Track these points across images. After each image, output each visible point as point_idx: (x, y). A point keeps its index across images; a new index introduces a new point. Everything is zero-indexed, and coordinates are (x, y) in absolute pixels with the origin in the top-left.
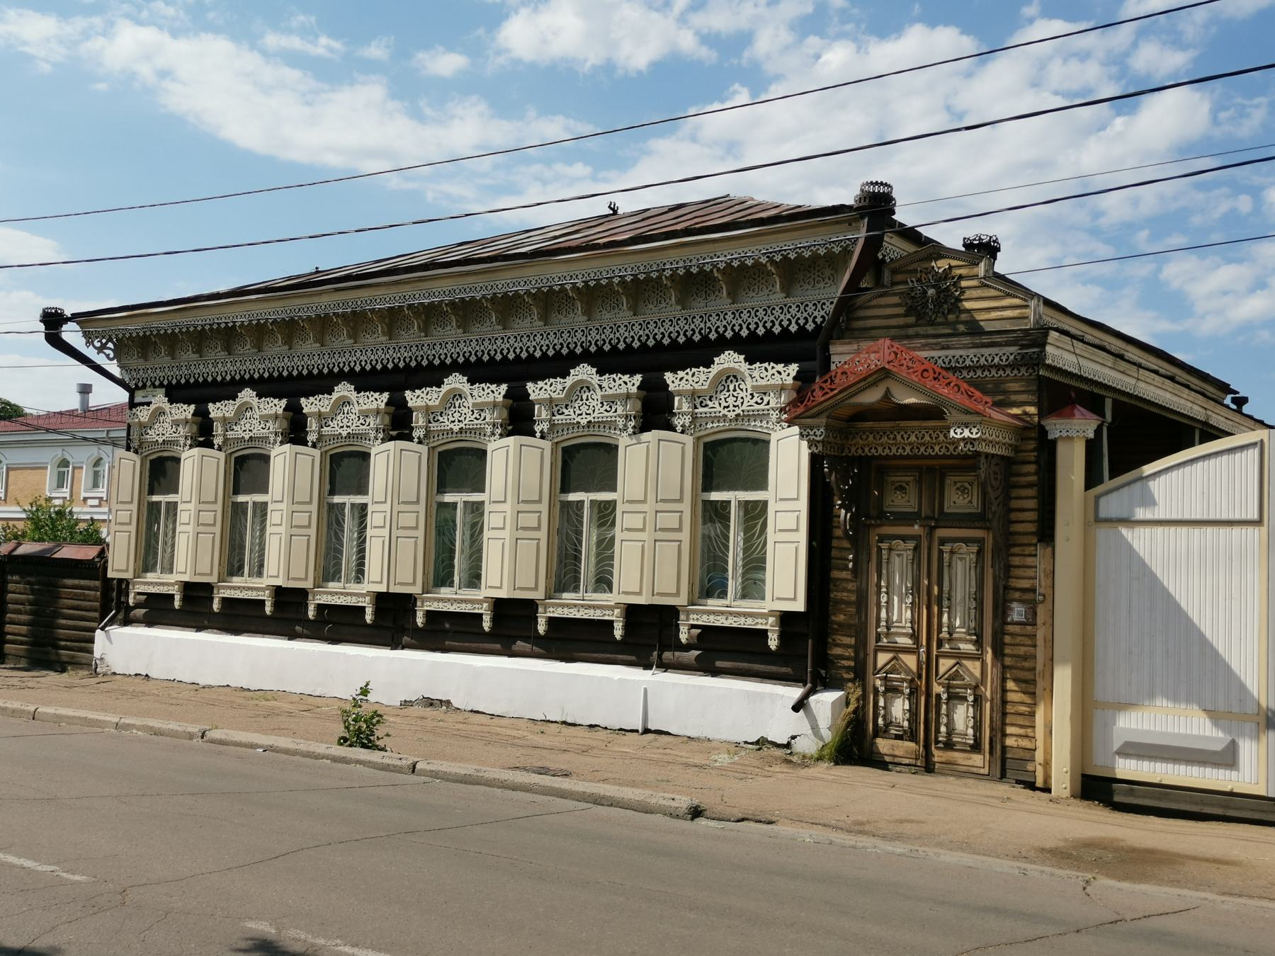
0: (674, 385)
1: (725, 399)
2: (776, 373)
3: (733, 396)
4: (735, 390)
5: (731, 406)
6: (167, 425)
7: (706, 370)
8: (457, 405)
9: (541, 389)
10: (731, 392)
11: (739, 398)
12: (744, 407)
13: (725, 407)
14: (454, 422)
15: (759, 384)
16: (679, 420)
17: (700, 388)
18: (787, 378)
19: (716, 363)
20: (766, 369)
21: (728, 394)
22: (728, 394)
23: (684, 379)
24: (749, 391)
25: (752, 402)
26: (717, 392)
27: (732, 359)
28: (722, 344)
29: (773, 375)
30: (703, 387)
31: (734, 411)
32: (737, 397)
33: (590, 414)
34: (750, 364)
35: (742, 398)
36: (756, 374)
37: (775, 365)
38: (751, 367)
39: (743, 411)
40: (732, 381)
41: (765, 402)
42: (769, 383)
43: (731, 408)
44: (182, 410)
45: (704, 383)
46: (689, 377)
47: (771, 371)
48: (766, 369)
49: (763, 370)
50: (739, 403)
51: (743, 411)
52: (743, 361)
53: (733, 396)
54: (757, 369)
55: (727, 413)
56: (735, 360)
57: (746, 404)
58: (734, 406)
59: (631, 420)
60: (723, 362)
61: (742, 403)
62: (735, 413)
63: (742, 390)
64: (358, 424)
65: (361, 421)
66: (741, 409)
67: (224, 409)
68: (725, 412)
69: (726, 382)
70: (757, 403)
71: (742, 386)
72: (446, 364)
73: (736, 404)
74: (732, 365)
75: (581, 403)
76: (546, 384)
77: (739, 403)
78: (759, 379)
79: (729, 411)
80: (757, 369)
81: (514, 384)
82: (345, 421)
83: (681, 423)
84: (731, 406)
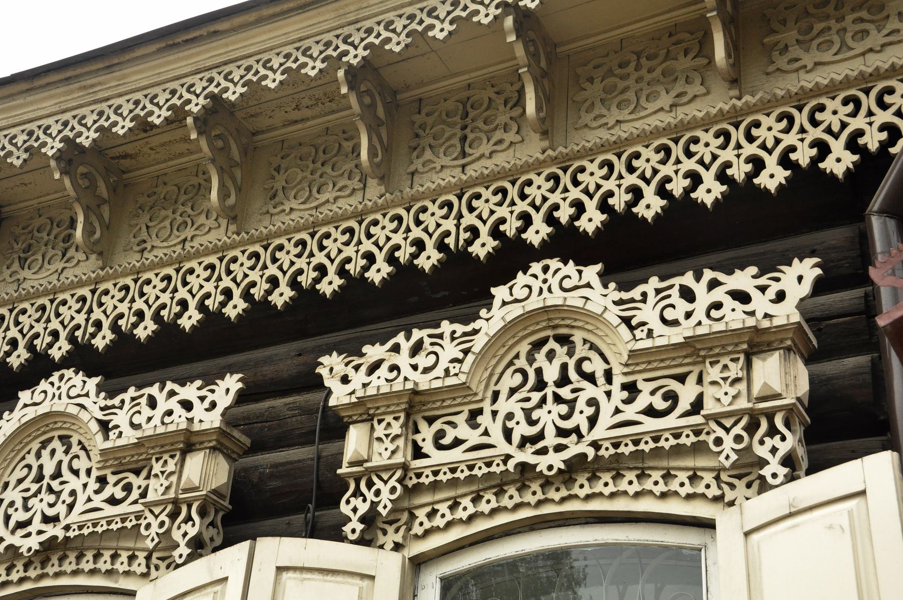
0: (349, 388)
1: (528, 413)
3: (558, 399)
4: (563, 381)
5: (550, 432)
7: (460, 329)
10: (549, 391)
11: (581, 404)
12: (600, 432)
13: (525, 441)
15: (660, 342)
17: (437, 384)
18: (773, 309)
19: (497, 303)
20: (688, 295)
21: (536, 397)
22: (536, 397)
23: (385, 367)
24: (618, 380)
25: (630, 412)
26: (496, 395)
27: (554, 282)
29: (718, 306)
30: (450, 381)
31: (559, 448)
32: (572, 403)
34: (624, 287)
36: (648, 314)
38: (625, 296)
39: (596, 445)
40: (551, 355)
41: (684, 404)
42: (701, 331)
43: (551, 439)
45: (454, 368)
46: (403, 360)
50: (580, 420)
51: (596, 445)
52: (596, 282)
53: (558, 399)
54: (652, 298)
56: (567, 284)
57: (606, 419)
58: (562, 433)
59: (189, 519)
61: (593, 421)
62: (567, 454)
63: (590, 378)
68: (527, 456)
69: (531, 360)
70: (650, 412)
71: (595, 366)
73: (568, 425)
74: (556, 298)
77: (580, 420)
79: (543, 451)
80: (652, 298)
83: (363, 508)
84: (550, 432)
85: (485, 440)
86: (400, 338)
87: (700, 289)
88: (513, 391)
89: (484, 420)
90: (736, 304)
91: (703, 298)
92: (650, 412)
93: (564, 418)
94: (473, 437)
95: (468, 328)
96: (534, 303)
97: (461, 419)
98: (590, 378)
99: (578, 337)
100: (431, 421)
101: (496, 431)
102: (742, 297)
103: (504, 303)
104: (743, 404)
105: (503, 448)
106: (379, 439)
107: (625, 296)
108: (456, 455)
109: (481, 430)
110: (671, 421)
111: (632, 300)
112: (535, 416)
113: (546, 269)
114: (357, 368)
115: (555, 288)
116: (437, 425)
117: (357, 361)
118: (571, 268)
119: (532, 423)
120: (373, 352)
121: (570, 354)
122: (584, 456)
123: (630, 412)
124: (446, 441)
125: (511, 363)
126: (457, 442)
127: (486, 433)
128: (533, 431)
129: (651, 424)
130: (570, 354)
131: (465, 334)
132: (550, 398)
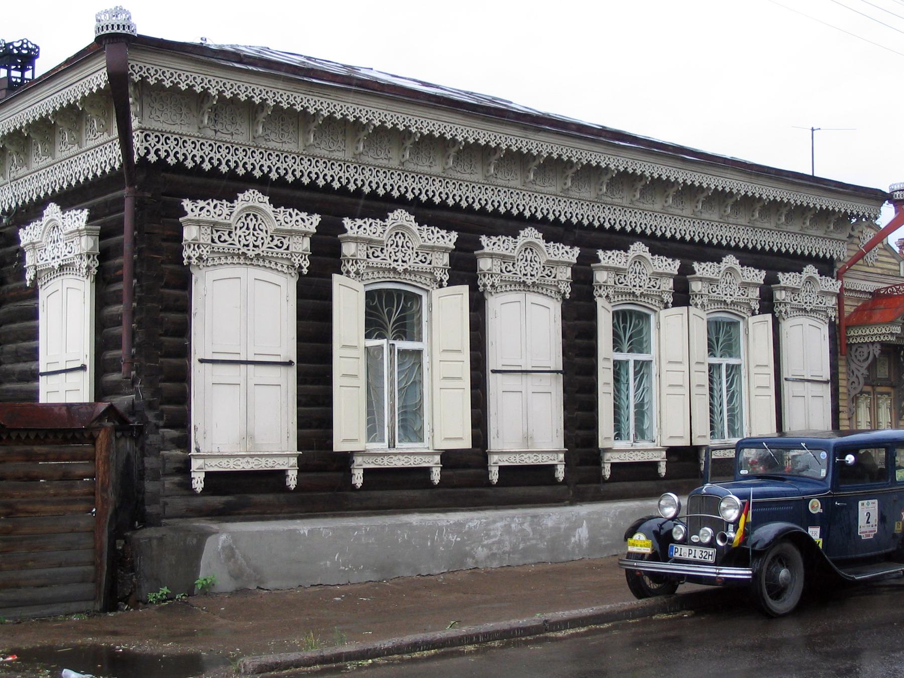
2: (300, 220)
6: (537, 265)
7: (229, 205)
8: (251, 227)
9: (359, 227)
11: (260, 238)
13: (244, 245)
14: (248, 246)
16: (353, 267)
19: (240, 199)
20: (291, 215)
26: (236, 228)
28: (248, 181)
32: (257, 238)
33: (258, 246)
35: (262, 239)
36: (280, 217)
37: (299, 213)
38: (276, 210)
42: (293, 228)
44: (754, 274)
45: (228, 217)
46: (211, 208)
48: (291, 215)
52: (268, 202)
55: (247, 252)
60: (247, 199)
63: (262, 230)
64: (417, 260)
65: (547, 272)
66: (409, 264)
67: (212, 210)
72: (348, 191)
74: (257, 204)
75: (248, 232)
76: (365, 223)
81: (466, 235)
82: (529, 269)
83: (197, 255)
84: (251, 245)
85: (233, 242)
86: (210, 201)
87: (294, 214)
89: (233, 235)
90: (302, 222)
91: (295, 218)
92: (276, 246)
93: (256, 241)
95: (232, 205)
96: (251, 204)
98: (262, 230)
100: (217, 231)
101: (237, 240)
102: (303, 220)
103: (242, 200)
104: (301, 251)
105: (238, 246)
106: (203, 234)
107: (276, 210)
108: (225, 245)
109: (232, 239)
110: (281, 250)
111: (276, 212)
112: (247, 238)
113: (254, 192)
114: (196, 207)
115: (257, 200)
116: (219, 233)
117: (196, 205)
118: (260, 195)
119: (247, 240)
120: (201, 203)
121: (257, 221)
122: (259, 254)
123: (272, 245)
124: (222, 239)
125: (240, 219)
126: (225, 241)
127: (233, 240)
129: (277, 250)
130: (257, 221)
131: (230, 207)
132: (251, 234)
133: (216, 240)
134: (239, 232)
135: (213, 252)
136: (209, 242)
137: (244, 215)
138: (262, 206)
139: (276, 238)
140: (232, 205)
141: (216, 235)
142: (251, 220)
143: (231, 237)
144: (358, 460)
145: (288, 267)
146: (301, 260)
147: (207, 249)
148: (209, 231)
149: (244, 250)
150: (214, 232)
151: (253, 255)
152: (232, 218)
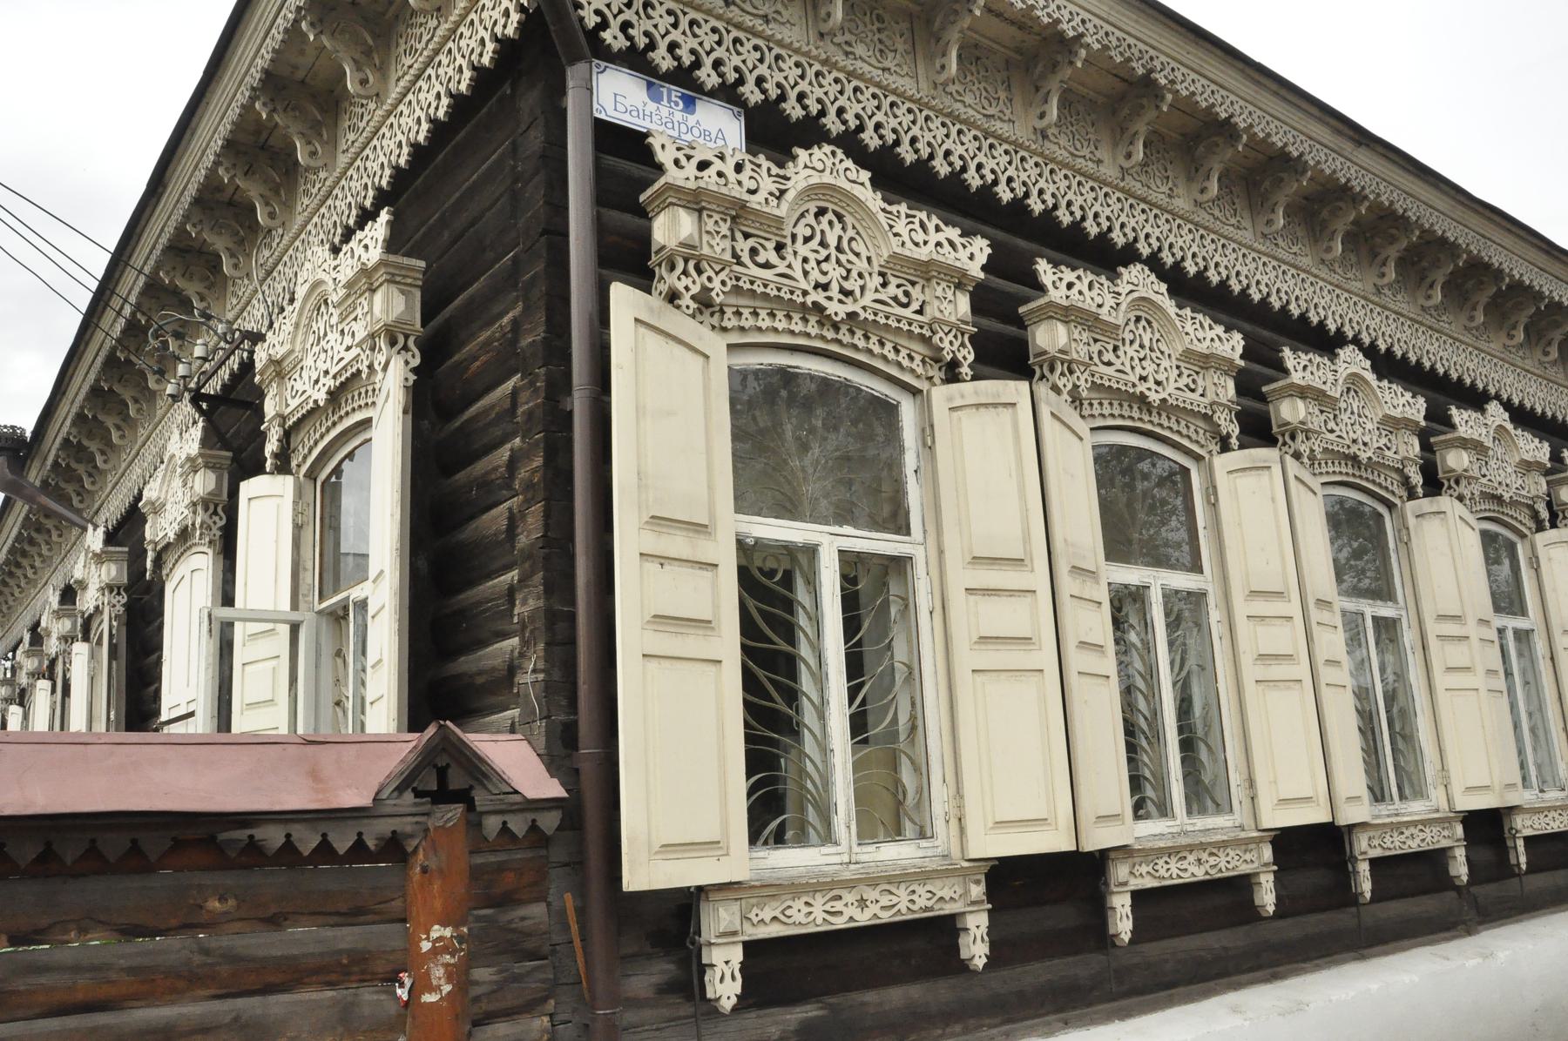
2: (946, 244)
5: (835, 287)
7: (775, 170)
11: (854, 274)
13: (817, 286)
15: (908, 253)
32: (849, 271)
36: (901, 226)
37: (942, 226)
38: (889, 208)
47: (934, 237)
49: (917, 226)
52: (868, 184)
60: (820, 166)
63: (857, 255)
74: (843, 183)
78: (909, 244)
83: (695, 289)
84: (835, 287)
85: (788, 271)
87: (931, 227)
88: (807, 240)
90: (951, 249)
94: (782, 269)
96: (827, 178)
97: (771, 245)
98: (857, 255)
99: (849, 219)
100: (747, 236)
103: (806, 166)
105: (803, 285)
106: (708, 232)
107: (889, 208)
109: (786, 263)
111: (890, 213)
116: (751, 242)
124: (761, 259)
125: (802, 215)
127: (789, 266)
128: (823, 280)
131: (778, 176)
132: (833, 259)
133: (746, 258)
134: (803, 250)
135: (737, 290)
136: (728, 256)
137: (813, 210)
138: (857, 191)
139: (894, 281)
140: (781, 172)
141: (744, 246)
142: (830, 223)
143: (783, 258)
144: (1120, 872)
145: (923, 361)
146: (957, 344)
147: (723, 276)
148: (724, 229)
149: (818, 297)
150: (739, 236)
151: (842, 315)
152: (785, 206)
